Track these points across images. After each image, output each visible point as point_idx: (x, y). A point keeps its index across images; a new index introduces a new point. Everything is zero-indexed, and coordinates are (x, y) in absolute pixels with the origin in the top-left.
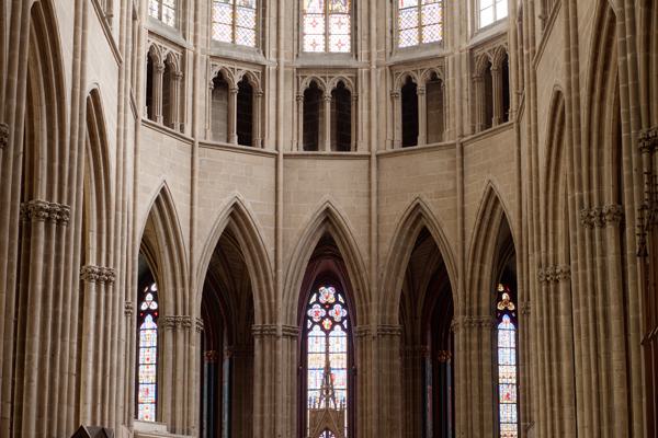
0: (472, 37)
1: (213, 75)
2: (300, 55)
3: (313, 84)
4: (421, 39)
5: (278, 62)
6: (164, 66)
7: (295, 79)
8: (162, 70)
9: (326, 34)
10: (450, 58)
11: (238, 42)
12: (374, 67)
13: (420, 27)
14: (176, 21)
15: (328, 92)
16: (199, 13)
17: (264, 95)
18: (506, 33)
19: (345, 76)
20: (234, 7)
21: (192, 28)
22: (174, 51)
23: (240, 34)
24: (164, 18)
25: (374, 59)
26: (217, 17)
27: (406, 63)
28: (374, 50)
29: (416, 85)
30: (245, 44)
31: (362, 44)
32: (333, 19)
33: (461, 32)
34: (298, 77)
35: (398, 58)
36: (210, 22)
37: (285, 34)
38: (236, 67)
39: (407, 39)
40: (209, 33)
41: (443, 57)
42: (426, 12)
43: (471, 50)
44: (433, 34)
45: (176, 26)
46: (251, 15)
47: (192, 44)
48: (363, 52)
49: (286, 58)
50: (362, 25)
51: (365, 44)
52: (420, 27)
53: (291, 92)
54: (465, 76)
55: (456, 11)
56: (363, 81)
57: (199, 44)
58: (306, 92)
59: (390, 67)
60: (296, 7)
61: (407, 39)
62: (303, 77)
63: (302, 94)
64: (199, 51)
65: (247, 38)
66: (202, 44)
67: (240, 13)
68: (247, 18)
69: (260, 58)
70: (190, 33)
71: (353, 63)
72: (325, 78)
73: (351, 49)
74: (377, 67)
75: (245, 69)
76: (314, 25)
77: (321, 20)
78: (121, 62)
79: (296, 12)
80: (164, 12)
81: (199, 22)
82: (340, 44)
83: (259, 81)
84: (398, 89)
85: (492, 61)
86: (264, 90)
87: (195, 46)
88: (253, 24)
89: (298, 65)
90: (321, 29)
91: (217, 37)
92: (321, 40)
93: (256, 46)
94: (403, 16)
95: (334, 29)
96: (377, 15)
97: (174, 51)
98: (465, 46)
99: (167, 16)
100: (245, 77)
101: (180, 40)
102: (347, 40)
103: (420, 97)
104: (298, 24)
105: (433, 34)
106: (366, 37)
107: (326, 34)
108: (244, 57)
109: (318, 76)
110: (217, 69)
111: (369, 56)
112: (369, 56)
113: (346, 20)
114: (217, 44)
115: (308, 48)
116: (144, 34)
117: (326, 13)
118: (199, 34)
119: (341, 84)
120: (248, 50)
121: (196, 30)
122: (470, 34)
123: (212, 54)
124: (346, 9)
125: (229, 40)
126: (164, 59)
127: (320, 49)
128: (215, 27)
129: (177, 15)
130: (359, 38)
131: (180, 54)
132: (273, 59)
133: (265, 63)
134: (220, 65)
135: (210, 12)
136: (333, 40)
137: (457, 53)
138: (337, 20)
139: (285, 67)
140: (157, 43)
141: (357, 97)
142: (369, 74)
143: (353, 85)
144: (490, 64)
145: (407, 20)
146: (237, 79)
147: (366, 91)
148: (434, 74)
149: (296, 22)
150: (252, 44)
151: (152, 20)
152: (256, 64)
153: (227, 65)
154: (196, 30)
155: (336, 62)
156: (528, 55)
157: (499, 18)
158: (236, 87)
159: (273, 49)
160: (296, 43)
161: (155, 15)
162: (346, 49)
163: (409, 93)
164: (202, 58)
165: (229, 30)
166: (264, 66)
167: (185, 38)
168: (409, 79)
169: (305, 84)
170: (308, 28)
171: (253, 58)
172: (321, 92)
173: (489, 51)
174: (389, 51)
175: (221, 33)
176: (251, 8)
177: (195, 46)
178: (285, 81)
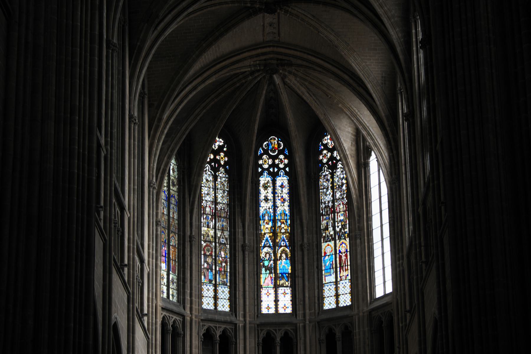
0: (371, 303)
1: (203, 332)
2: (259, 315)
3: (269, 334)
4: (337, 302)
5: (245, 320)
6: (171, 329)
7: (256, 332)
8: (171, 332)
9: (276, 301)
10: (357, 317)
11: (220, 308)
12: (307, 322)
13: (337, 296)
14: (178, 297)
15: (278, 340)
16: (194, 292)
17: (236, 343)
18: (391, 303)
19: (289, 328)
20: (215, 286)
21: (189, 302)
22: (178, 318)
23: (220, 303)
24: (171, 296)
25: (307, 317)
26: (205, 293)
27: (328, 320)
28: (307, 311)
29: (335, 334)
30: (223, 309)
31: (300, 307)
32: (281, 290)
33: (363, 300)
34: (258, 330)
35: (323, 317)
36: (200, 296)
37: (249, 302)
38: (218, 326)
39: (329, 304)
40: (201, 303)
41: (352, 316)
42: (340, 286)
43: (371, 312)
44: (346, 300)
45: (178, 301)
46: (227, 290)
47: (189, 312)
48: (300, 313)
49: (250, 318)
50: (299, 296)
51: (301, 307)
52: (337, 296)
53: (254, 341)
54: (366, 329)
55: (360, 286)
56: (301, 332)
57: (194, 312)
58: (264, 340)
59: (318, 322)
60: (256, 284)
61: (329, 304)
62: (262, 330)
63: (261, 340)
64: (194, 317)
65: (224, 306)
66: (196, 312)
67: (220, 289)
68: (224, 292)
69: (233, 318)
70: (188, 306)
71: (294, 320)
72: (276, 330)
73: (293, 310)
74: (310, 322)
75: (223, 326)
76: (268, 294)
77: (272, 291)
78: (148, 338)
79: (256, 287)
80: (171, 293)
81: (194, 298)
82: (285, 307)
83: (233, 334)
84: (323, 337)
85: (383, 320)
86: (236, 340)
87: (191, 313)
88: (228, 296)
89: (258, 322)
90: (272, 297)
91: (205, 306)
92: (272, 305)
93: (230, 311)
94: (326, 288)
95: (281, 297)
96: (309, 288)
97: (178, 318)
98: (365, 309)
99: (173, 295)
100: (224, 332)
101: (181, 310)
102: (289, 304)
103: (338, 342)
104: (257, 295)
105: (346, 300)
106: (302, 303)
107: (276, 301)
108: (222, 319)
109: (272, 329)
110: (205, 328)
111: (304, 315)
112: (304, 315)
113: (288, 291)
114: (206, 311)
115: (264, 311)
116: (159, 308)
117: (276, 287)
118: (194, 306)
119: (286, 333)
120: (224, 313)
121: (191, 303)
122: (369, 302)
123: (202, 318)
124: (288, 284)
125: (212, 307)
126: (171, 324)
127: (272, 311)
128: (204, 300)
129: (178, 294)
130: (297, 303)
131: (181, 320)
132: (241, 319)
133: (237, 322)
134: (207, 325)
135: (200, 290)
136: (281, 304)
137: (361, 314)
138: (283, 291)
139: (249, 324)
140: (167, 314)
141: (297, 343)
142: (304, 327)
143: (294, 334)
144: (382, 322)
145: (329, 291)
146: (218, 333)
147: (303, 338)
148: (346, 327)
149: (256, 293)
150: (227, 309)
151: (163, 299)
152: (231, 323)
153: (212, 325)
154: (191, 303)
155: (283, 320)
156: (402, 327)
157: (387, 292)
158: (218, 339)
159: (242, 313)
160: (256, 307)
161: (165, 295)
162: (289, 310)
163: (330, 338)
164: (196, 321)
165: (212, 301)
166: (236, 324)
167: (185, 310)
168: (331, 330)
169: (262, 335)
170: (264, 297)
171: (228, 319)
172: (273, 340)
173: (381, 314)
174: (317, 312)
175: (208, 304)
176: (226, 285)
177: (191, 313)
178: (250, 333)
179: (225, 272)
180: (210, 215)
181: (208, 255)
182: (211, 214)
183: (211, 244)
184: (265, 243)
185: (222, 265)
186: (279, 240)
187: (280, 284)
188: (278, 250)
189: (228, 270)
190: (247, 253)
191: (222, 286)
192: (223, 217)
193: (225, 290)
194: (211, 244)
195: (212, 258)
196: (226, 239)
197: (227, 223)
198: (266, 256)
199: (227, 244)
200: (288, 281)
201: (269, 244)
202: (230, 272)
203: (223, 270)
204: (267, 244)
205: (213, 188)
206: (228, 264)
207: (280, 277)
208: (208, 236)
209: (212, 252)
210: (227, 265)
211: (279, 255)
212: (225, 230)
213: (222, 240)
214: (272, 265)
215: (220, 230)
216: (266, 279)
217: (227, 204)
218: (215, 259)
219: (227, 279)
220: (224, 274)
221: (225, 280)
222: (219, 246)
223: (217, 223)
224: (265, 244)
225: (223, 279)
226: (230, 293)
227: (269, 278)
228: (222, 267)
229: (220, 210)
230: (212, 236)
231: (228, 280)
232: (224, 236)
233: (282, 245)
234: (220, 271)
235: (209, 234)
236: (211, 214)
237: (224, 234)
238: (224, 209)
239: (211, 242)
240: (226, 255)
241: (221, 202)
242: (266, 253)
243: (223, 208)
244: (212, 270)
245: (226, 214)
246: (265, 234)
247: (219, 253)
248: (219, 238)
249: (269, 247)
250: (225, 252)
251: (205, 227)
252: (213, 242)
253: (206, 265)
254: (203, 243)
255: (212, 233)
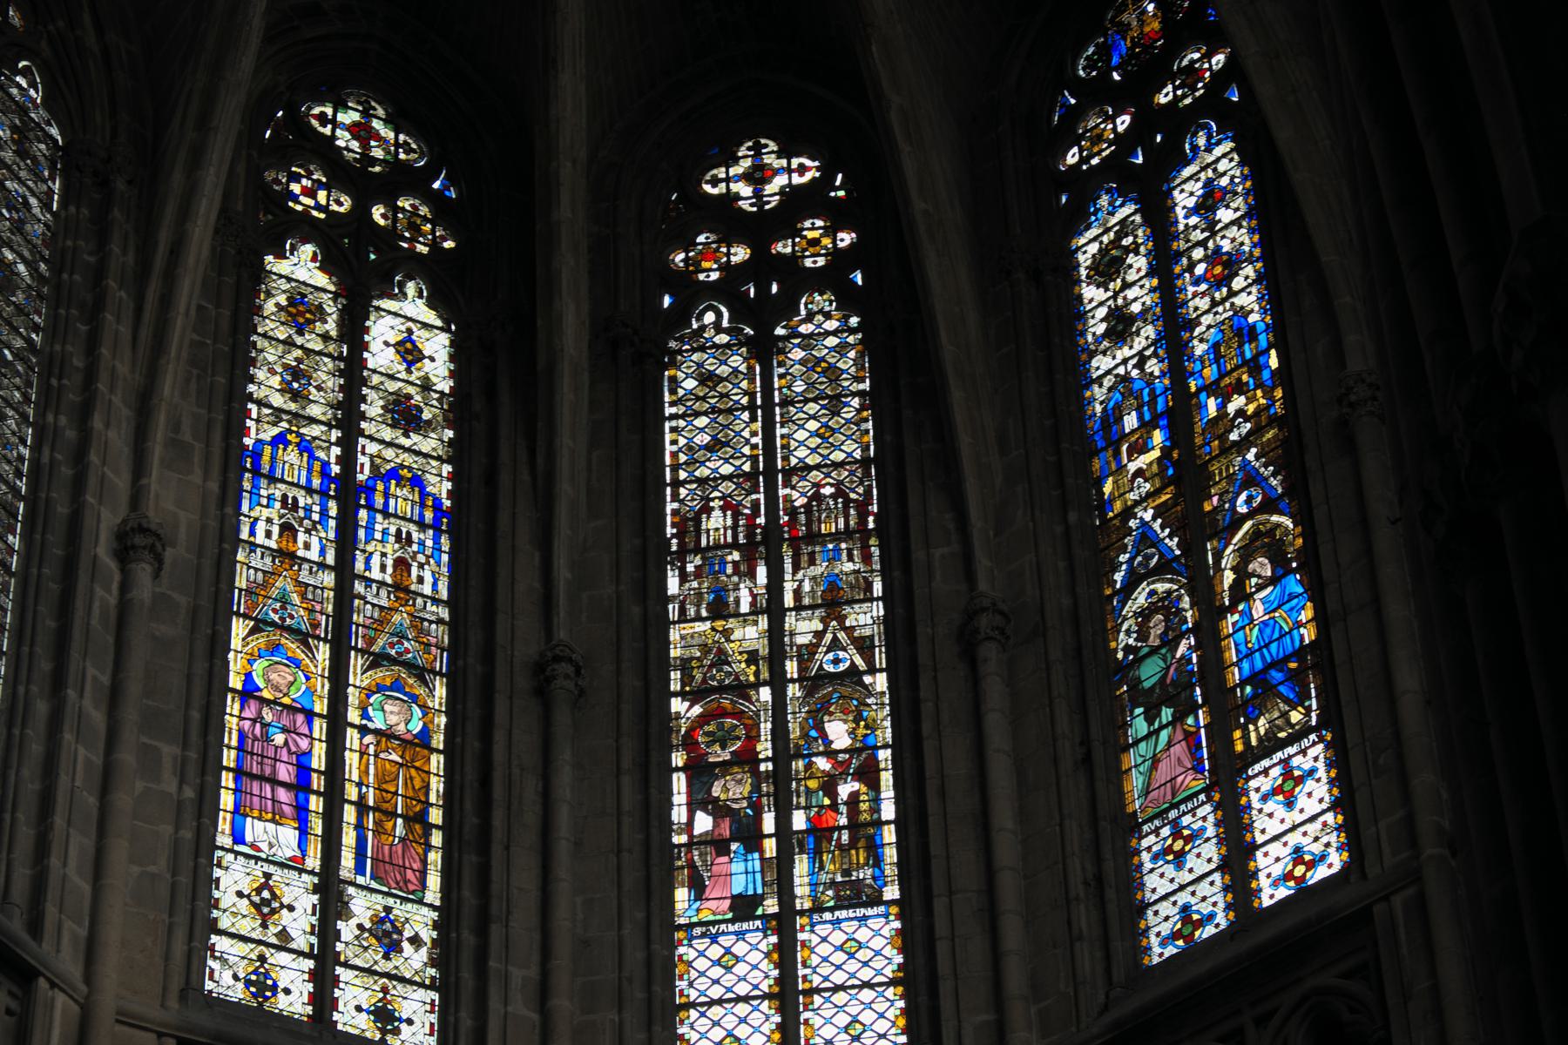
20: (784, 925)
176: (876, 900)
179: (864, 832)
180: (735, 545)
181: (724, 763)
182: (742, 540)
183: (749, 699)
184: (1130, 561)
185: (833, 794)
186: (1221, 495)
187: (1254, 742)
188: (1218, 556)
189: (888, 811)
190: (990, 653)
191: (842, 914)
192: (837, 537)
193: (863, 935)
194: (749, 699)
195: (755, 772)
196: (864, 646)
197: (867, 558)
198: (1143, 635)
199: (872, 670)
200: (1301, 698)
201: (1162, 556)
202: (899, 822)
203: (843, 821)
204: (1148, 558)
205: (752, 407)
206: (887, 778)
207: (1247, 702)
208: (722, 659)
209: (753, 738)
210: (874, 786)
211: (1229, 577)
212: (851, 602)
213: (831, 656)
214: (1189, 661)
215: (812, 607)
216: (1155, 761)
217: (865, 462)
218: (781, 776)
219: (877, 861)
220: (853, 843)
221: (866, 874)
222: (809, 693)
223: (788, 577)
224: (1131, 571)
225: (846, 873)
226: (906, 940)
227: (1179, 750)
228: (834, 807)
229: (808, 507)
230: (752, 658)
231: (890, 871)
232: (841, 635)
233: (1242, 509)
234: (820, 832)
235: (729, 647)
236: (742, 540)
237: (841, 619)
238: (840, 492)
239: (742, 689)
240: (861, 731)
241: (813, 460)
242: (1145, 615)
243: (828, 491)
244: (752, 840)
245: (852, 512)
246: (1128, 512)
247: (805, 735)
248: (806, 655)
249: (1165, 568)
250: (856, 721)
251: (698, 618)
252: (757, 685)
253: (703, 823)
254: (677, 705)
255: (751, 635)
